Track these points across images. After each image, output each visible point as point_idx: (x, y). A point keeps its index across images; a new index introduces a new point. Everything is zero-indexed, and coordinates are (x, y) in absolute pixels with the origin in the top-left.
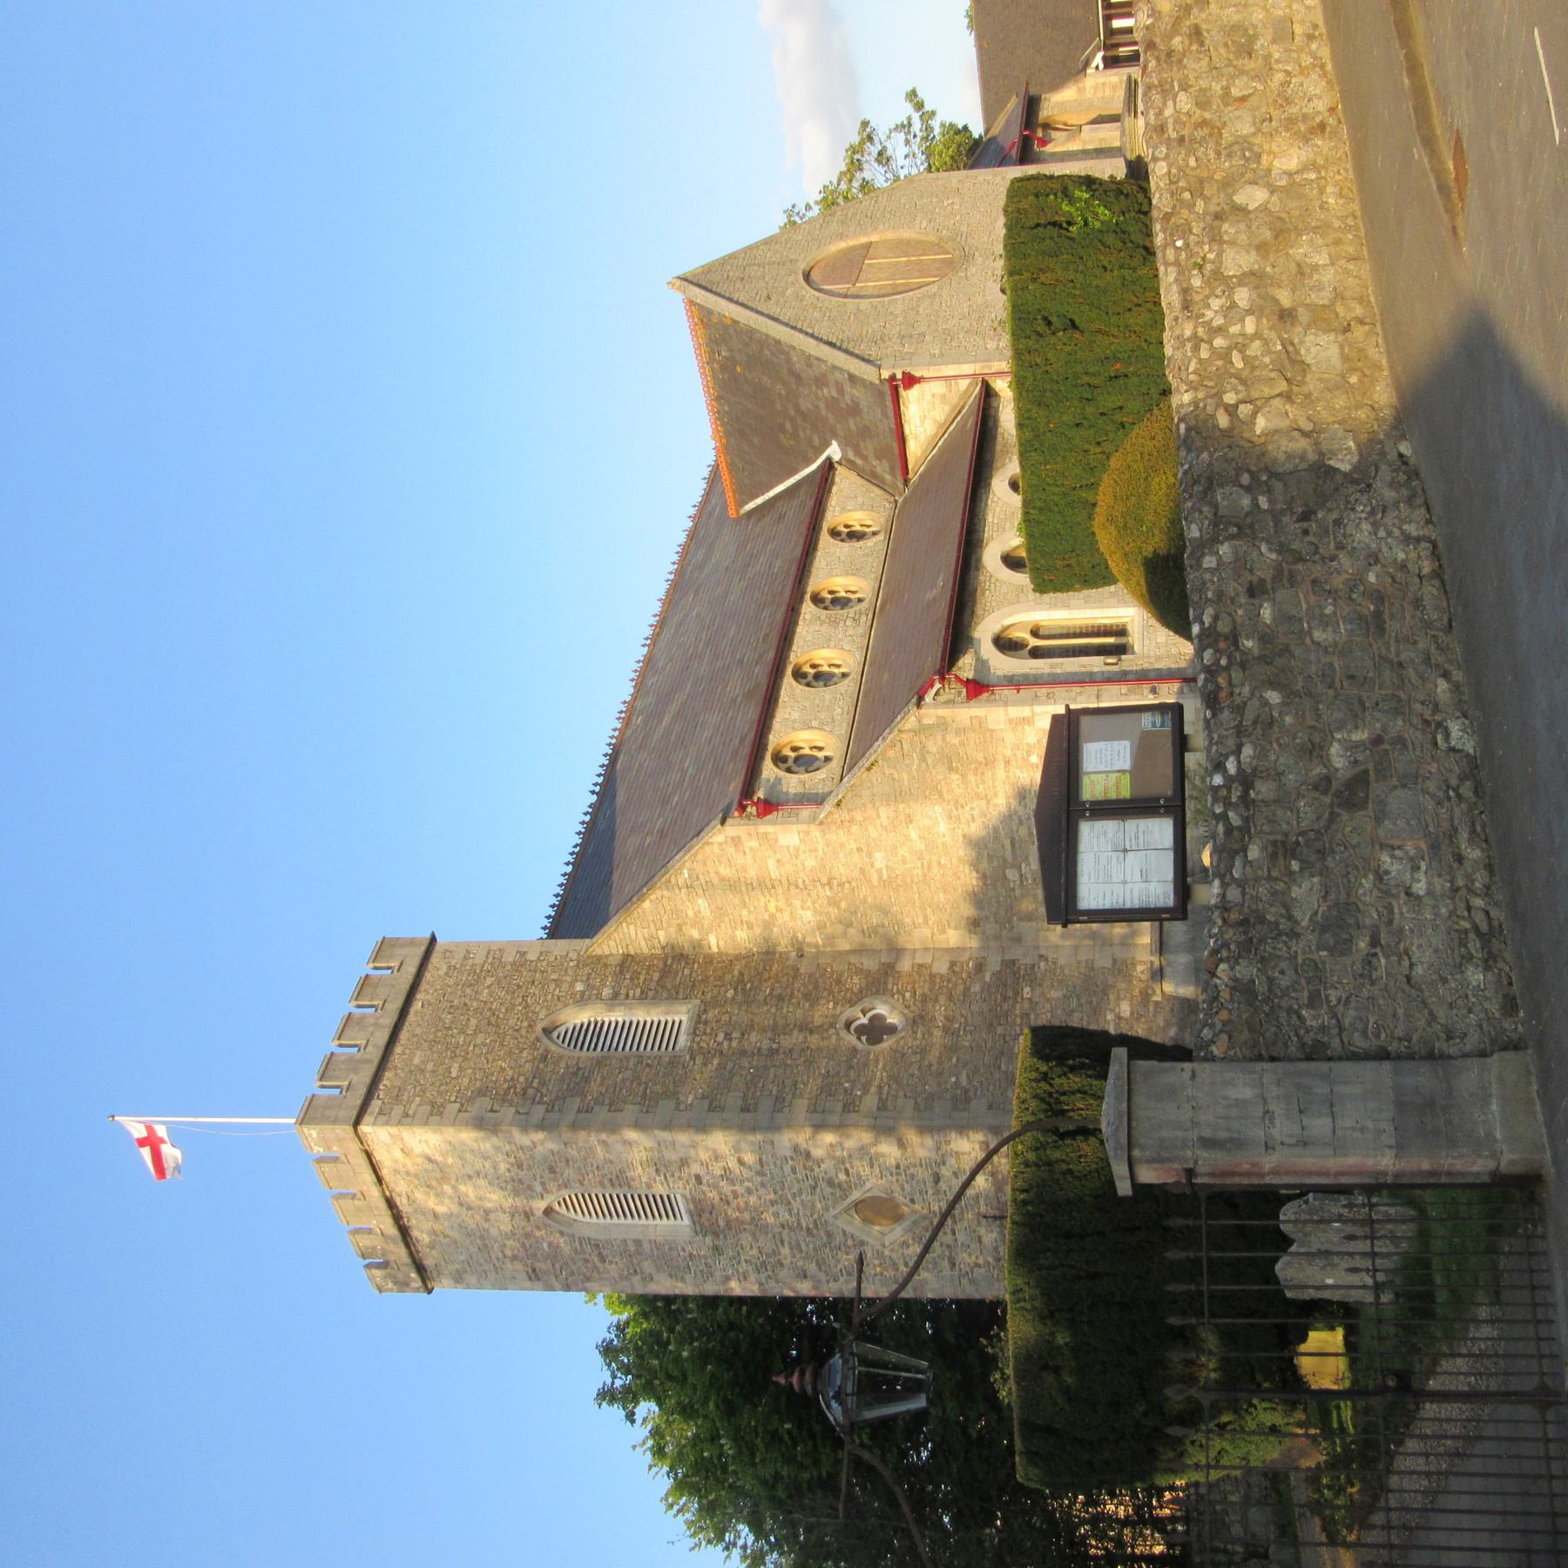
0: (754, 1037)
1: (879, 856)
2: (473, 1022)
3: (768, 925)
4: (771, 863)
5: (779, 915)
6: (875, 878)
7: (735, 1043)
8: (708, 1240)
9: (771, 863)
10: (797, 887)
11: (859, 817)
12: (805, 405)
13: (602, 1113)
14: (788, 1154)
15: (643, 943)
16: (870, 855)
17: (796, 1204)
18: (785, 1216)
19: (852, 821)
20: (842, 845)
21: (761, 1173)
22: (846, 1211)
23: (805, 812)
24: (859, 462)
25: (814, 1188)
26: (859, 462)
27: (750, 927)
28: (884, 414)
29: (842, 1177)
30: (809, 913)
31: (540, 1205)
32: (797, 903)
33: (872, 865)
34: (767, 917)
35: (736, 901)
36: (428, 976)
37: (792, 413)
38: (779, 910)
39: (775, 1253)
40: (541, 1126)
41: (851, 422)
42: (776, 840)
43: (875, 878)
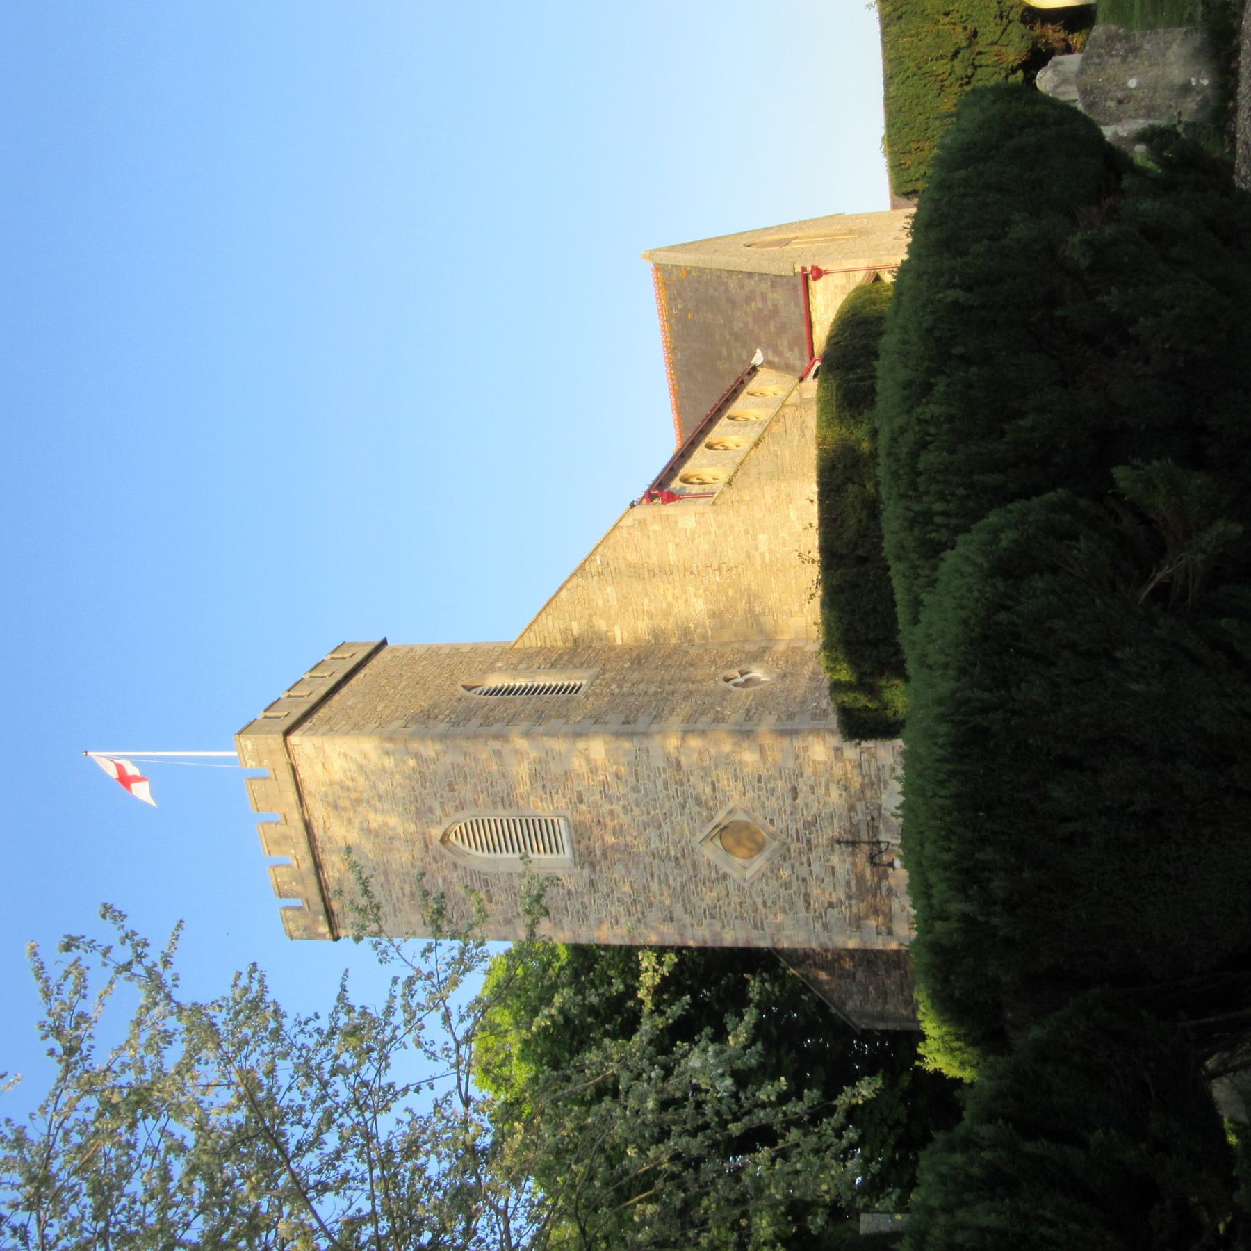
0: (642, 687)
1: (762, 537)
2: (404, 683)
3: (667, 614)
4: (671, 547)
5: (675, 603)
6: (758, 561)
7: (625, 690)
8: (586, 871)
9: (671, 547)
10: (692, 573)
11: (747, 498)
12: (738, 325)
13: (496, 727)
14: (661, 764)
15: (558, 635)
16: (755, 539)
17: (666, 828)
18: (655, 843)
19: (741, 501)
20: (732, 527)
21: (636, 789)
22: (709, 838)
23: (703, 500)
24: (776, 360)
25: (683, 806)
26: (776, 360)
27: (651, 617)
28: (797, 305)
29: (708, 790)
30: (701, 601)
31: (437, 832)
32: (691, 590)
33: (757, 549)
34: (664, 605)
35: (639, 588)
36: (374, 661)
37: (728, 337)
38: (675, 598)
39: (646, 889)
40: (443, 737)
41: (772, 325)
42: (676, 522)
43: (758, 561)
